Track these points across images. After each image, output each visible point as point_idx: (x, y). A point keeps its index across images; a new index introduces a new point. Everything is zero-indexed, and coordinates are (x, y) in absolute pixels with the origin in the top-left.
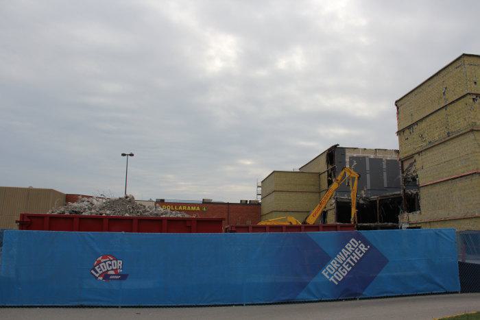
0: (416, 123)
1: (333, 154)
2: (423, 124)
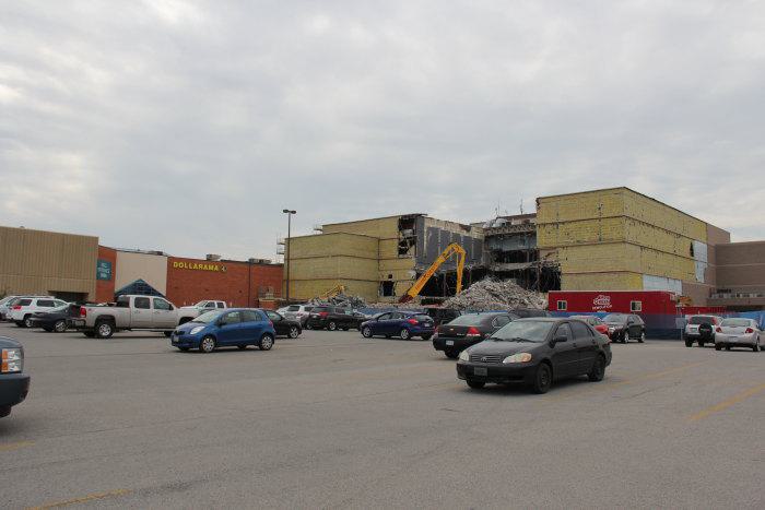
0: (563, 223)
1: (407, 222)
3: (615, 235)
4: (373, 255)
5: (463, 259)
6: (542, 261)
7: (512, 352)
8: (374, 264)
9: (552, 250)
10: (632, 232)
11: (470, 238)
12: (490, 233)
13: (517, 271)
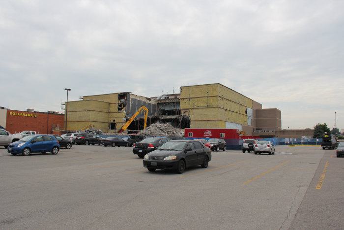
1: (122, 96)
2: (196, 100)
3: (214, 104)
4: (106, 111)
5: (147, 113)
6: (182, 115)
7: (168, 155)
8: (106, 115)
9: (187, 110)
10: (221, 103)
11: (150, 104)
12: (160, 102)
13: (171, 119)
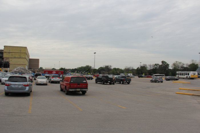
3: (24, 57)
6: (5, 61)
7: (6, 81)
